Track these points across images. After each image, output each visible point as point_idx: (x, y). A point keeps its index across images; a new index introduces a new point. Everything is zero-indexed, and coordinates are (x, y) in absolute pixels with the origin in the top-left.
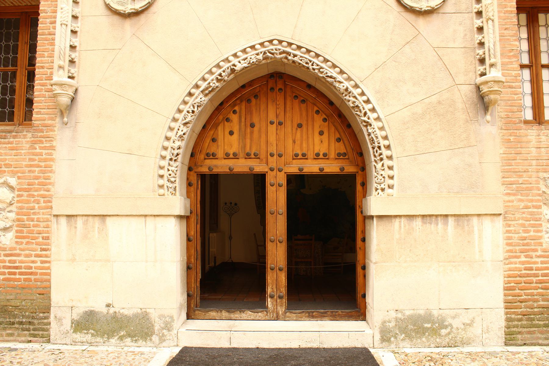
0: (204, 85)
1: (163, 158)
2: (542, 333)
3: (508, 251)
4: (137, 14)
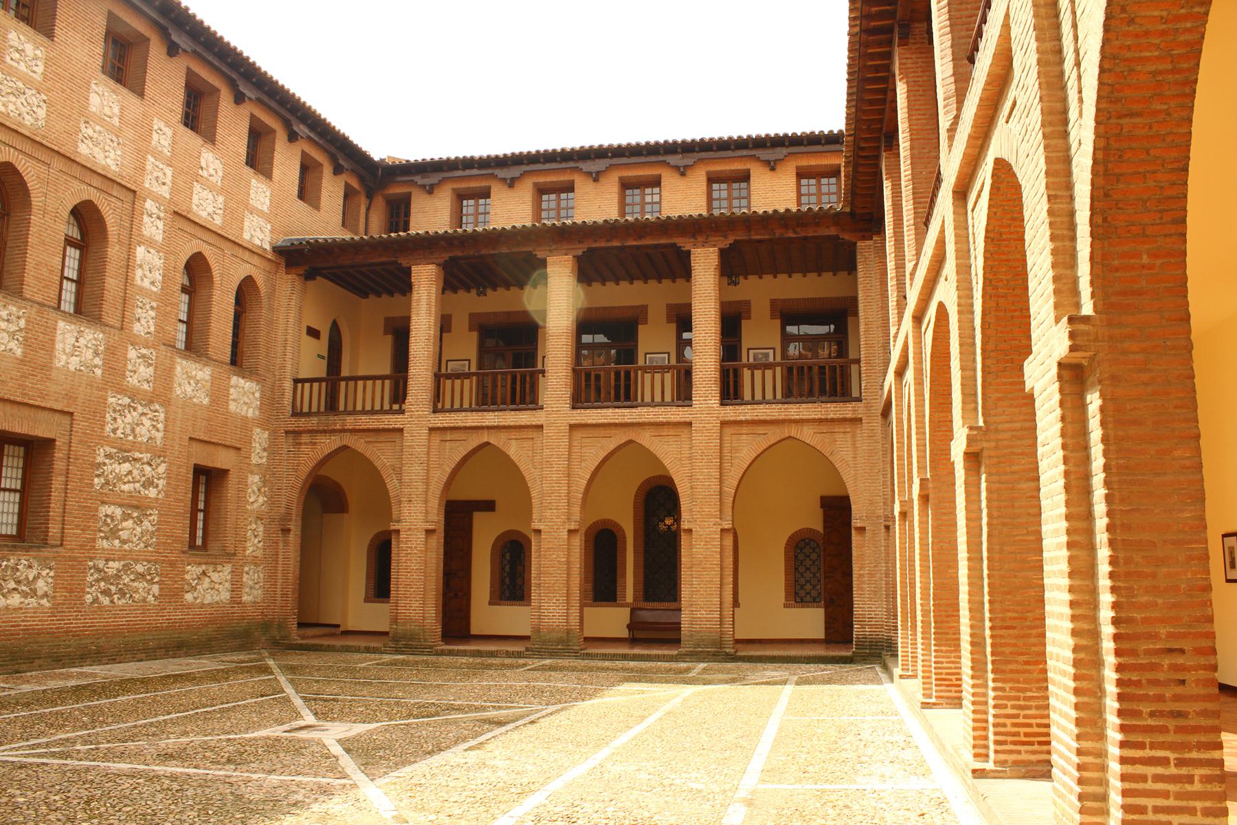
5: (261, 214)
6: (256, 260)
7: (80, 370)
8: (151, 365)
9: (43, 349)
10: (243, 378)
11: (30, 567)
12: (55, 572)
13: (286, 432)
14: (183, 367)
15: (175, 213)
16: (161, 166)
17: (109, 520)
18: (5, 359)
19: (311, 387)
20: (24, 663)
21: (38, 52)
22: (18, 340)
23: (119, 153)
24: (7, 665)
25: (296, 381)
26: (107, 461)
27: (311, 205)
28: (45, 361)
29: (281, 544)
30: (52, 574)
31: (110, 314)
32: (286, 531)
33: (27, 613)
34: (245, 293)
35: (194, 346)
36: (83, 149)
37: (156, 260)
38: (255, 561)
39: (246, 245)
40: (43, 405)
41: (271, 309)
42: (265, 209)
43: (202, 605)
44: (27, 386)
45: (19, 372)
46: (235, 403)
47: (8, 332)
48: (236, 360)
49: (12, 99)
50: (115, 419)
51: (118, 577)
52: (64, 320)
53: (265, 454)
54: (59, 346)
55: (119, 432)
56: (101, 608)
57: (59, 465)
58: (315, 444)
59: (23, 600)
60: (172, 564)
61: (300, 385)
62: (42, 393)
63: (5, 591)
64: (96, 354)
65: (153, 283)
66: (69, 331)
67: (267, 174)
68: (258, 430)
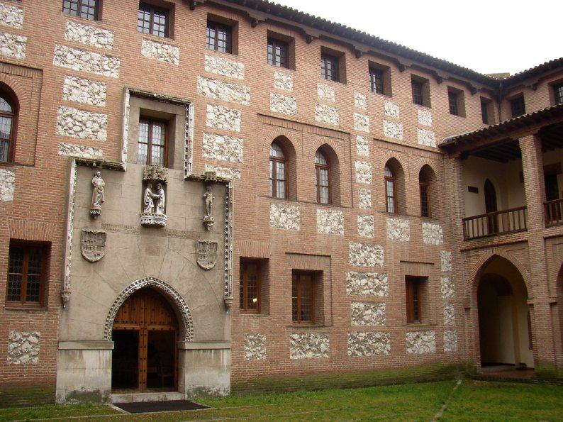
0: (124, 295)
1: (106, 325)
4: (96, 262)
5: (427, 128)
6: (429, 155)
8: (371, 224)
10: (430, 222)
13: (462, 251)
14: (390, 222)
15: (374, 139)
16: (362, 116)
17: (357, 311)
19: (473, 222)
21: (289, 78)
23: (338, 116)
25: (464, 220)
26: (352, 279)
27: (461, 116)
29: (466, 317)
30: (328, 341)
31: (345, 201)
32: (467, 309)
34: (425, 174)
35: (399, 211)
36: (318, 119)
37: (367, 167)
38: (450, 328)
39: (421, 148)
40: (314, 253)
41: (443, 181)
42: (430, 125)
43: (418, 355)
46: (426, 238)
48: (426, 213)
49: (280, 104)
50: (355, 256)
51: (365, 341)
53: (451, 265)
54: (319, 222)
55: (358, 263)
56: (357, 358)
57: (326, 283)
58: (478, 256)
60: (397, 332)
61: (466, 222)
64: (340, 223)
65: (367, 180)
67: (428, 105)
68: (444, 252)
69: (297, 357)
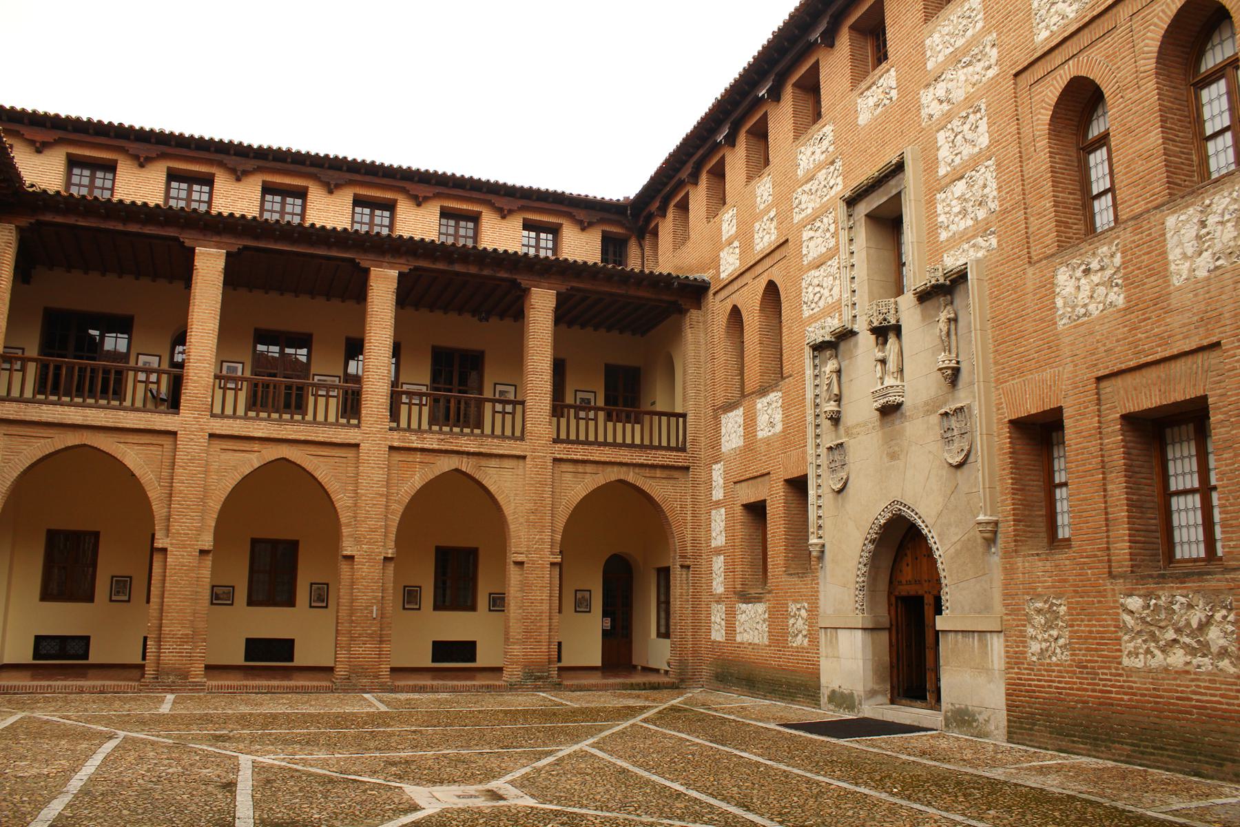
2: (1028, 735)
3: (1008, 663)
7: (1217, 268)
9: (1151, 275)
11: (1190, 606)
12: (1237, 614)
18: (1106, 320)
20: (1207, 763)
22: (1117, 285)
24: (1180, 758)
28: (1157, 289)
33: (1198, 680)
40: (1167, 354)
44: (1140, 340)
45: (1126, 326)
47: (1103, 284)
52: (1175, 212)
59: (1188, 658)
62: (1161, 339)
63: (1162, 643)
66: (1187, 221)
69: (1139, 663)
